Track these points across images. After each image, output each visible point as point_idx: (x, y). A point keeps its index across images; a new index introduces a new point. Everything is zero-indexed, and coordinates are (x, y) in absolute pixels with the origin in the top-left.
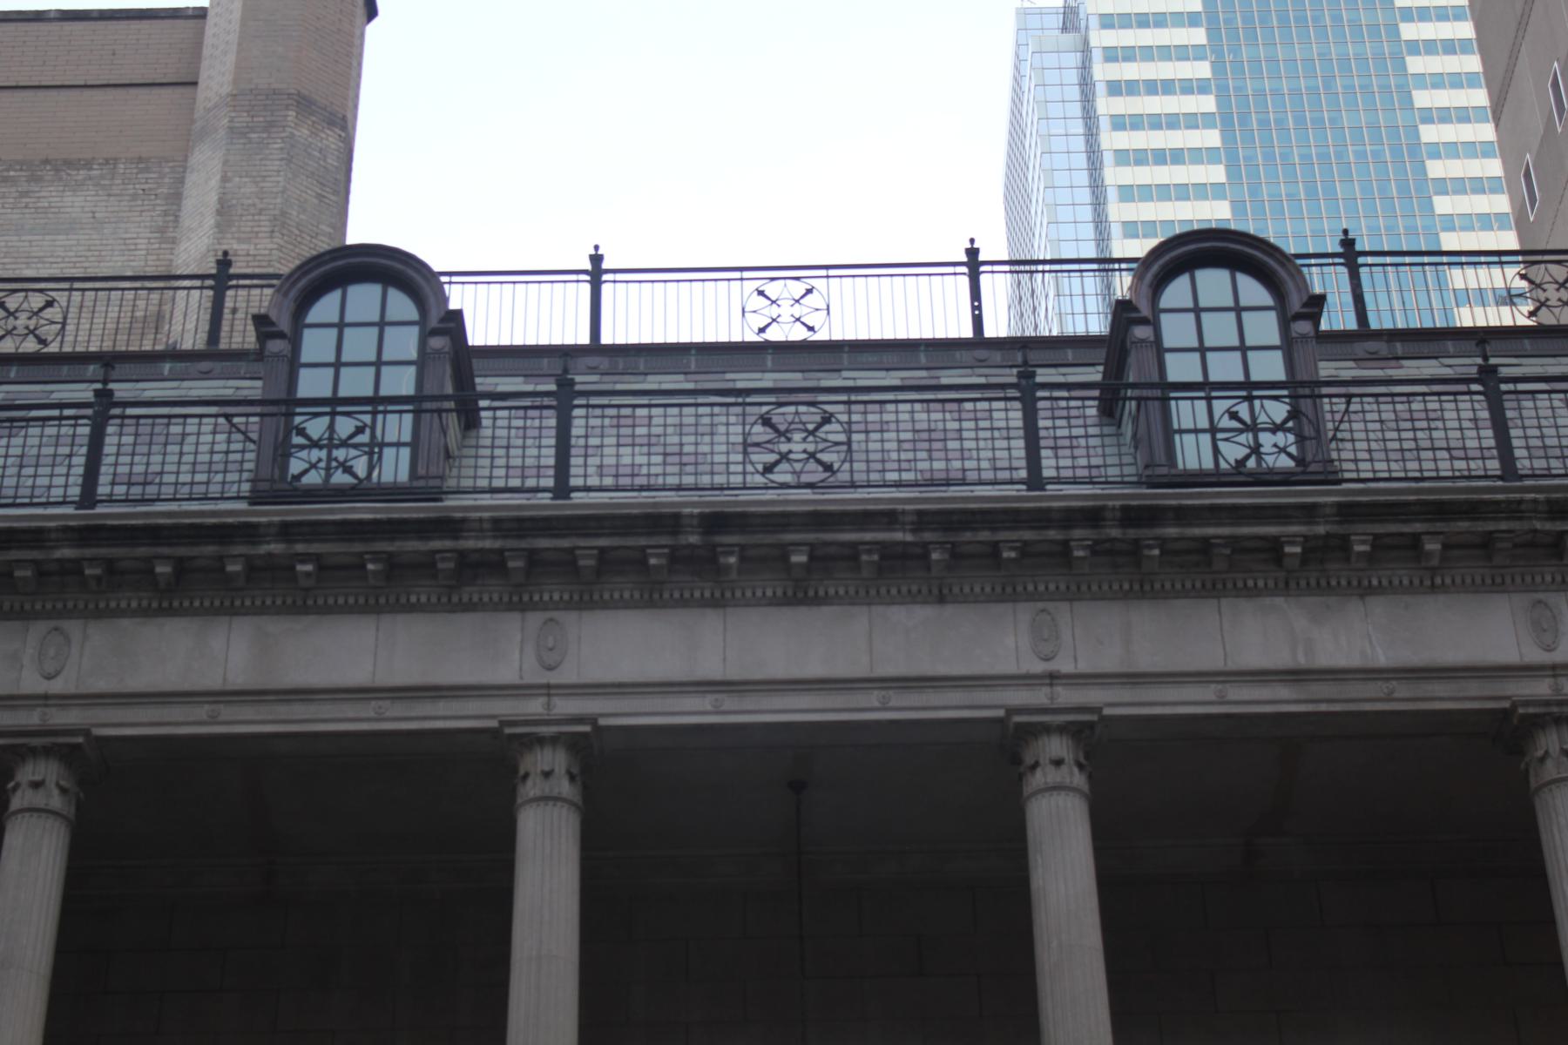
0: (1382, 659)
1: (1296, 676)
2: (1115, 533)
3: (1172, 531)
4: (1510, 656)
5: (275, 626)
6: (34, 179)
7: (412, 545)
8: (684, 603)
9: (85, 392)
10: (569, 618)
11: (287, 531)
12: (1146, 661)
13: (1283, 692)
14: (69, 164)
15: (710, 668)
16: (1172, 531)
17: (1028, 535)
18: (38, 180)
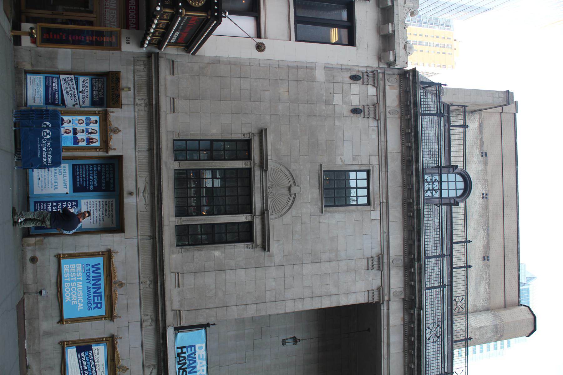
6: (486, 278)
14: (489, 285)
18: (486, 279)
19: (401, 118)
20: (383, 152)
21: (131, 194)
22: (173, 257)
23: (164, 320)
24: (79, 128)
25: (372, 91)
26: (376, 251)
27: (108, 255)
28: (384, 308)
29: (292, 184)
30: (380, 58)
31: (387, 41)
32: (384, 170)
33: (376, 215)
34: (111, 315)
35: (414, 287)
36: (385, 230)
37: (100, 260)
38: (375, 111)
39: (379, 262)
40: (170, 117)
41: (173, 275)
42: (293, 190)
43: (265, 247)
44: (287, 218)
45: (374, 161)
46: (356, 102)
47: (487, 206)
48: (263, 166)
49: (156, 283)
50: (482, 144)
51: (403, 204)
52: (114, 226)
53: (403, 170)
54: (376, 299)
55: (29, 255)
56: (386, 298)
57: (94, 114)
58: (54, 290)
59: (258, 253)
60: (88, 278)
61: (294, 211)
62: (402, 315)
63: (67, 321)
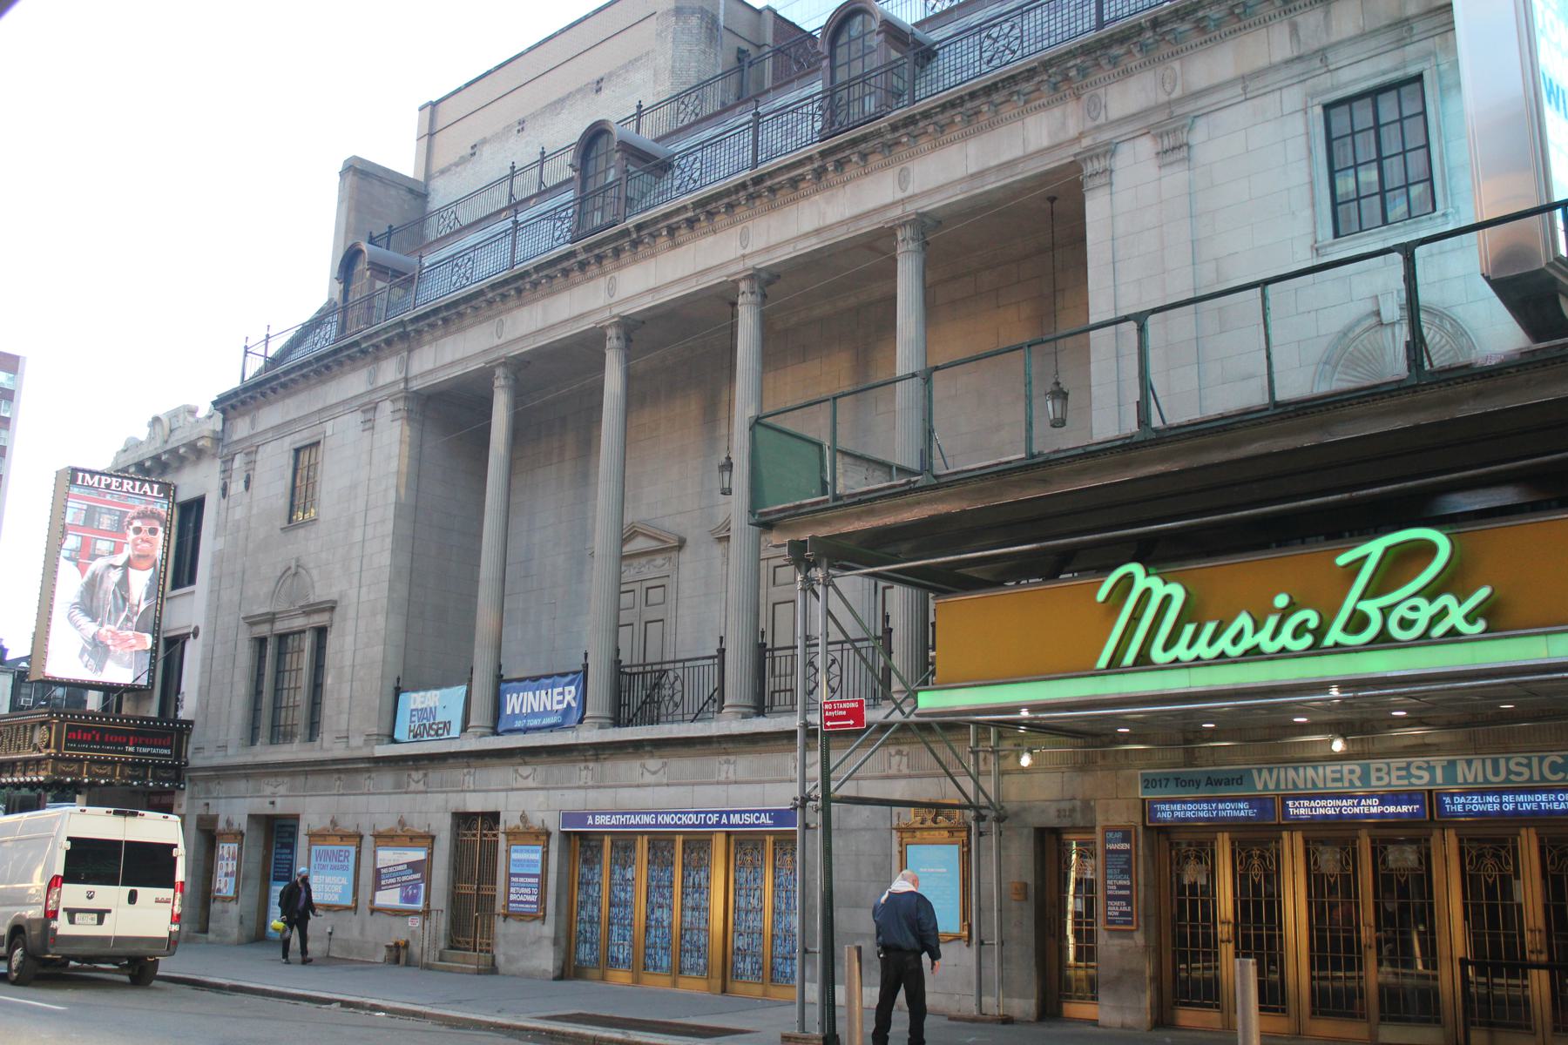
0: (848, 214)
1: (818, 232)
2: (751, 190)
3: (769, 183)
4: (889, 200)
5: (546, 302)
7: (565, 264)
8: (645, 258)
9: (509, 224)
10: (616, 274)
11: (588, 249)
12: (773, 240)
13: (814, 240)
15: (652, 284)
16: (769, 183)
17: (726, 200)
19: (258, 408)
20: (280, 430)
22: (329, 747)
23: (362, 760)
25: (239, 462)
26: (359, 416)
28: (416, 385)
30: (214, 456)
31: (195, 452)
33: (329, 427)
35: (389, 342)
38: (251, 453)
39: (369, 409)
40: (230, 751)
42: (293, 570)
43: (331, 607)
44: (315, 573)
46: (242, 484)
47: (534, 116)
48: (271, 618)
49: (338, 771)
50: (463, 161)
51: (323, 382)
53: (296, 393)
54: (401, 405)
56: (402, 386)
60: (324, 867)
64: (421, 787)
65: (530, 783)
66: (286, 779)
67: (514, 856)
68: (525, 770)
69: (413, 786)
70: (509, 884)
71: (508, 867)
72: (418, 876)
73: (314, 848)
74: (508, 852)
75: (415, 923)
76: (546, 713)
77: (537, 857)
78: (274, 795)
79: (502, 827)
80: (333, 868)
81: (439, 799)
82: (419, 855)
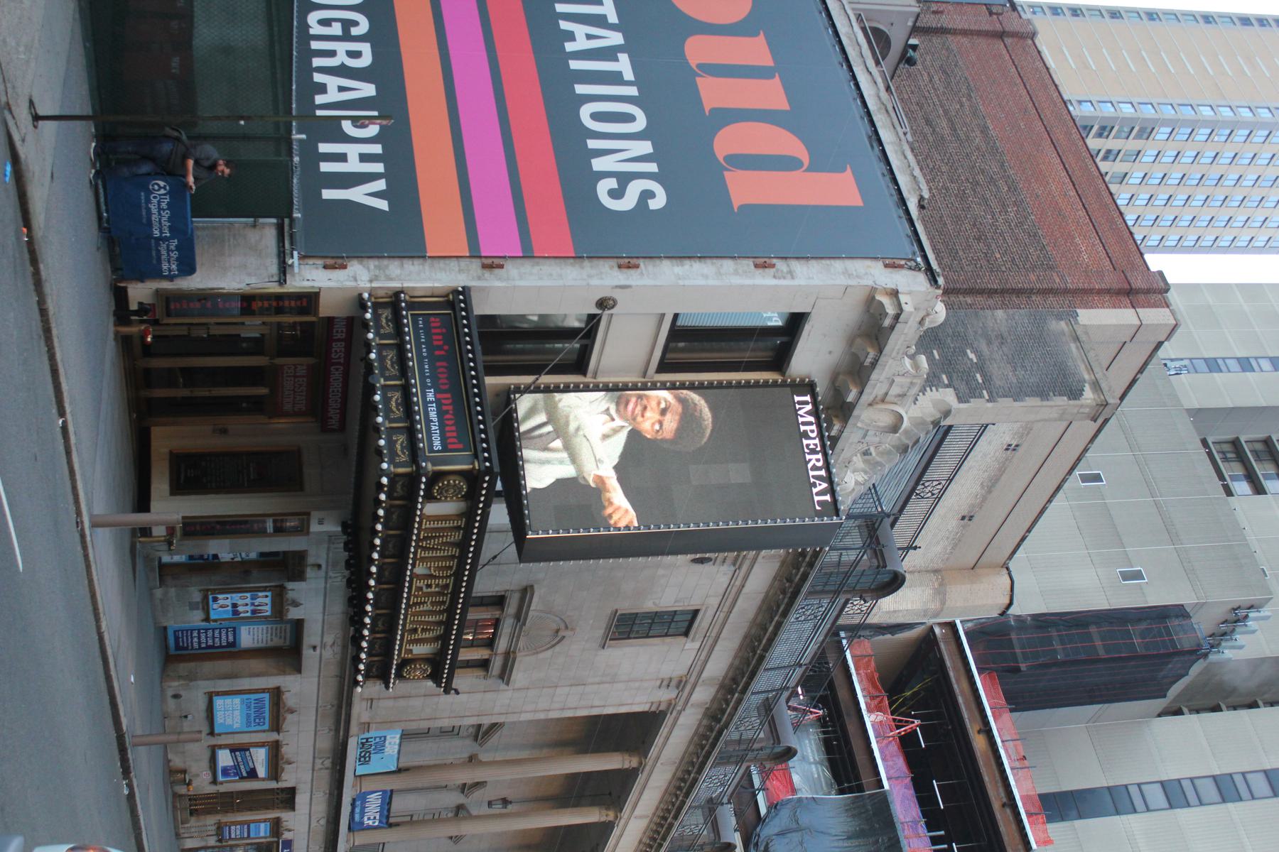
21: (314, 648)
24: (240, 602)
27: (277, 694)
29: (562, 626)
32: (725, 609)
34: (276, 726)
36: (703, 658)
37: (267, 696)
41: (364, 703)
42: (561, 634)
45: (714, 602)
49: (340, 707)
52: (288, 643)
54: (662, 707)
55: (170, 692)
57: (265, 589)
58: (203, 714)
59: (493, 682)
61: (557, 648)
62: (700, 717)
63: (220, 735)
64: (318, 766)
65: (314, 824)
66: (338, 657)
67: (262, 825)
68: (323, 822)
69: (318, 761)
70: (241, 823)
71: (254, 821)
72: (245, 774)
73: (267, 696)
74: (265, 821)
75: (206, 776)
76: (363, 814)
77: (262, 834)
78: (323, 646)
79: (285, 816)
80: (248, 716)
81: (307, 776)
82: (262, 772)
